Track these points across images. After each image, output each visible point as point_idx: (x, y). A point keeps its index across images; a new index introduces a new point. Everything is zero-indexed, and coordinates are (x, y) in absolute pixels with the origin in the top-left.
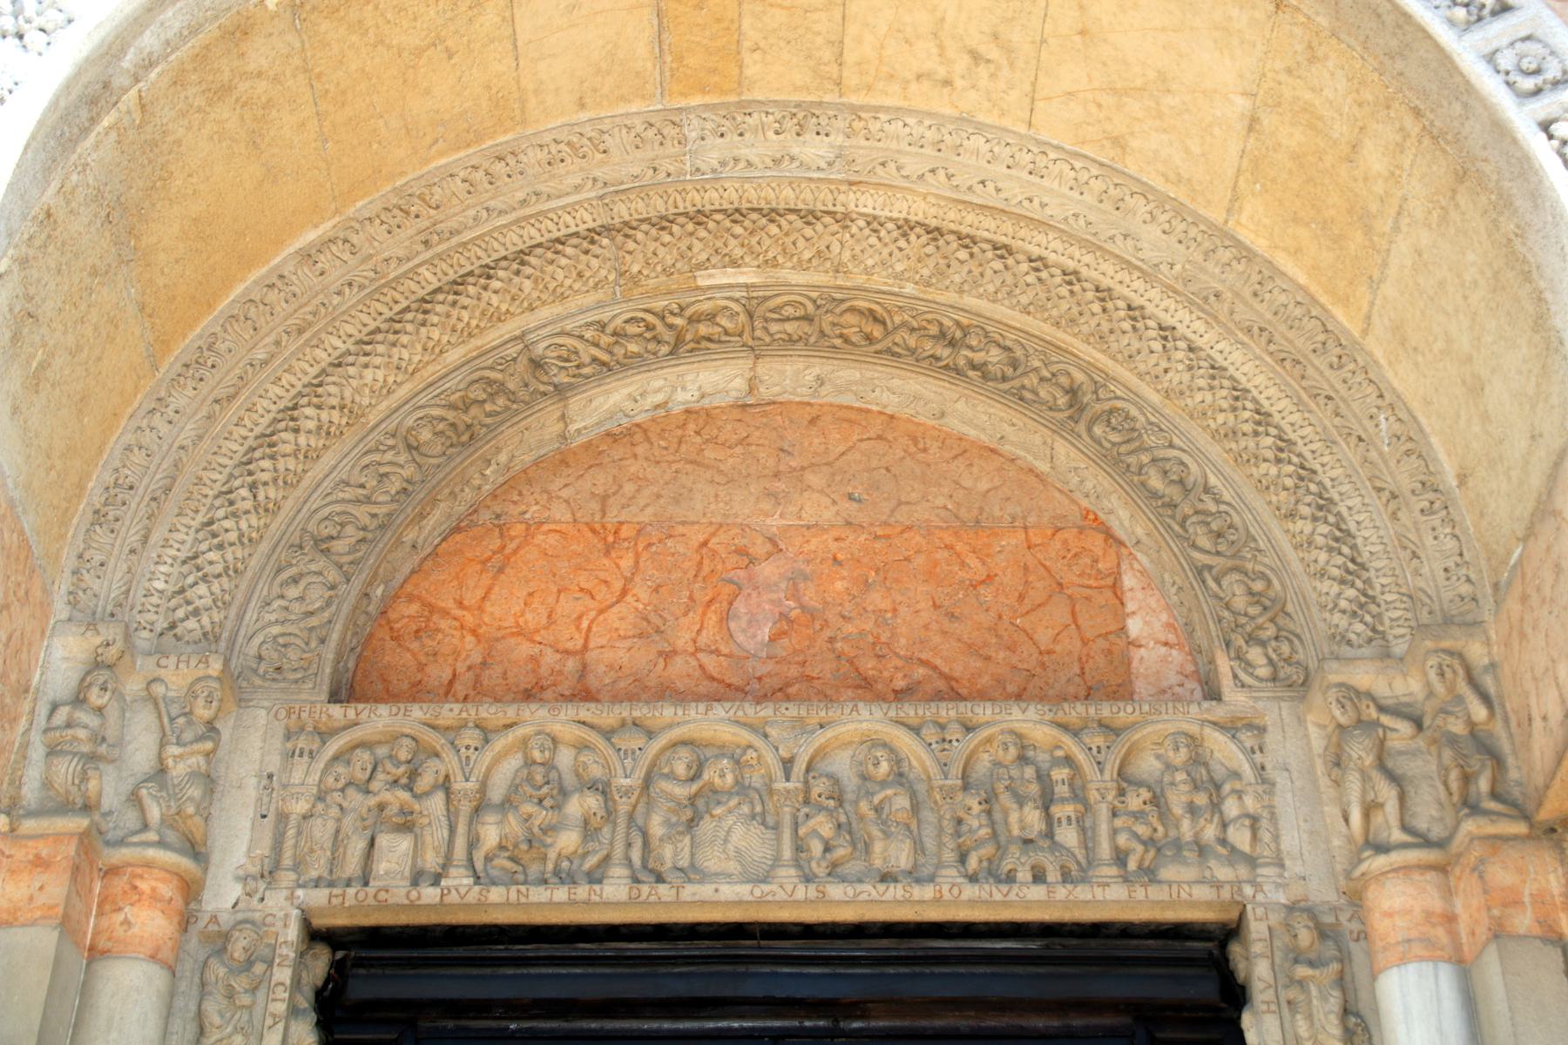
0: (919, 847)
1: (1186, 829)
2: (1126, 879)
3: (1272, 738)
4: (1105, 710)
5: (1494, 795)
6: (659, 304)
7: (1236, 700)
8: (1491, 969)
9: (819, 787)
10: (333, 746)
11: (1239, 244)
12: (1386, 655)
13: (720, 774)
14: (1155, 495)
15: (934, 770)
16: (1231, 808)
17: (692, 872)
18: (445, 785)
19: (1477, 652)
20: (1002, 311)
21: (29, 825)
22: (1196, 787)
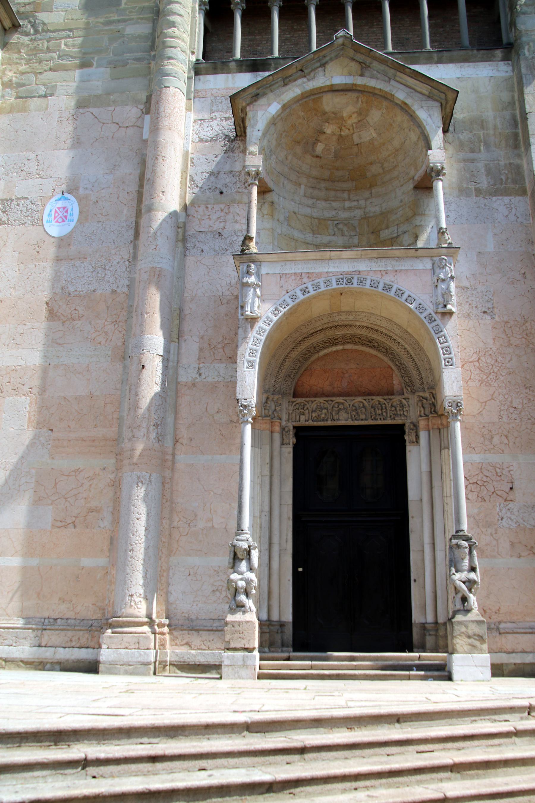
0: (366, 415)
1: (399, 413)
2: (391, 419)
3: (410, 400)
4: (390, 397)
5: (434, 411)
6: (330, 337)
7: (406, 395)
8: (431, 431)
9: (354, 408)
10: (294, 404)
11: (408, 332)
12: (424, 391)
13: (341, 407)
14: (397, 365)
15: (368, 406)
16: (405, 409)
17: (338, 420)
18: (308, 409)
19: (434, 392)
20: (377, 338)
21: (264, 418)
22: (400, 407)
